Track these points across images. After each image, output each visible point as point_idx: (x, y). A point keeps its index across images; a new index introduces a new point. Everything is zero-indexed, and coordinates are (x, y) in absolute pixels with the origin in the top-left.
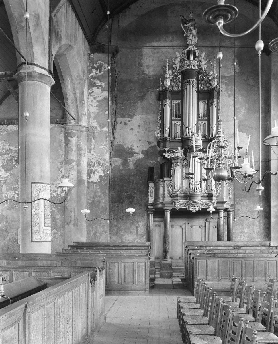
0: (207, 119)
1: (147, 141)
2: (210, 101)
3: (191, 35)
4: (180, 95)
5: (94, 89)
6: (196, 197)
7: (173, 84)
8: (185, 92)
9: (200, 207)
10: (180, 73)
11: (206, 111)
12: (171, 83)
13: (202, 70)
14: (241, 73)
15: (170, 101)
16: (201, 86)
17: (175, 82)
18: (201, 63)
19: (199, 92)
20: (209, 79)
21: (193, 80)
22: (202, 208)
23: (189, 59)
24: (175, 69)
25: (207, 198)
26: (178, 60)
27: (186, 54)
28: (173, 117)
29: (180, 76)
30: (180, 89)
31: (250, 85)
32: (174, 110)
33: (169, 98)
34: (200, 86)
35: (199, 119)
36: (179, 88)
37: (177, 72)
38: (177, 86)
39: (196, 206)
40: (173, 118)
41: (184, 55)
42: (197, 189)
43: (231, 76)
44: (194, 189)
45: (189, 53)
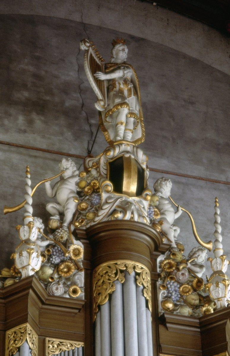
7: (49, 271)
8: (105, 309)
10: (76, 234)
16: (167, 298)
18: (162, 214)
19: (159, 320)
20: (195, 277)
23: (118, 188)
24: (57, 217)
26: (71, 186)
29: (78, 245)
30: (81, 294)
34: (160, 298)
36: (75, 292)
38: (69, 282)
41: (94, 172)
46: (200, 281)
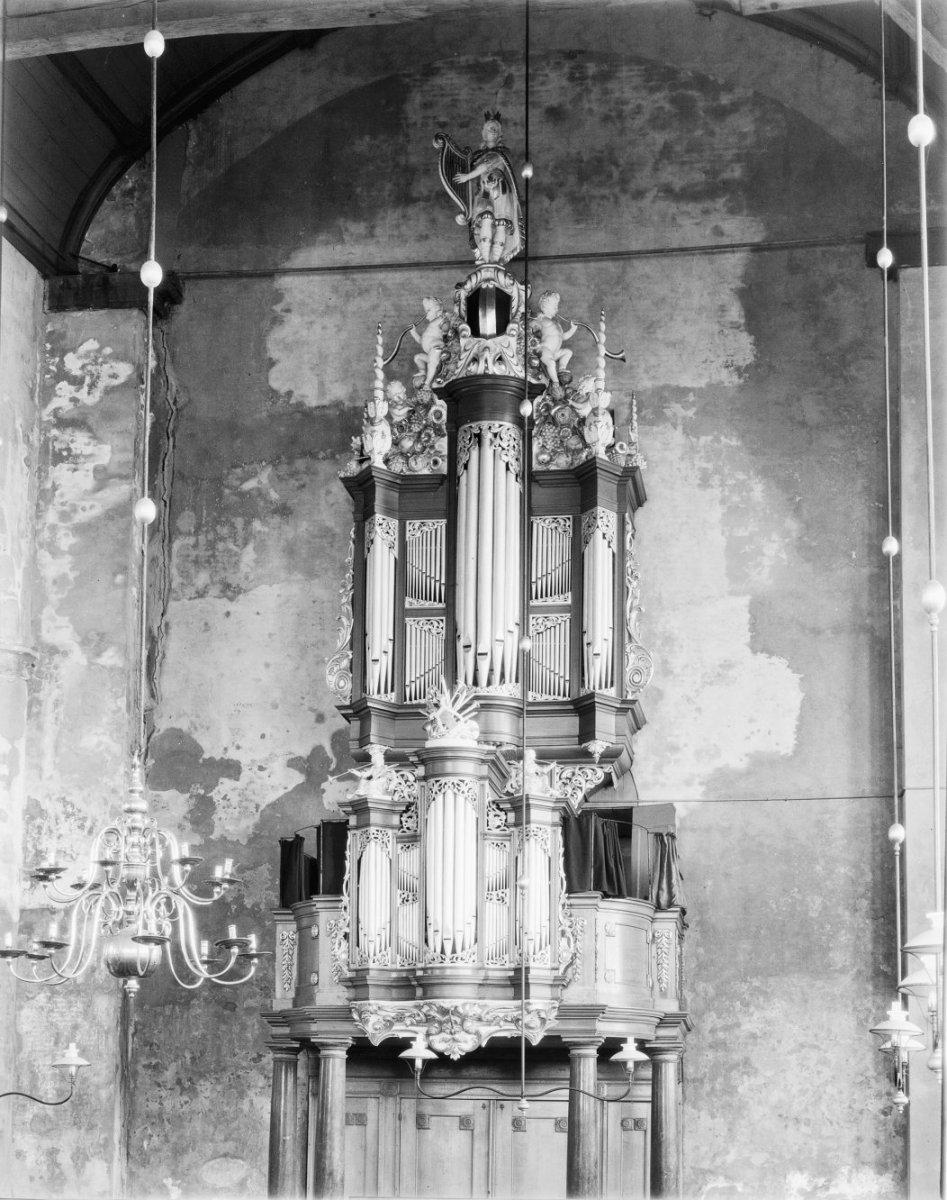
0: (569, 602)
1: (306, 707)
2: (585, 519)
3: (487, 222)
4: (438, 496)
5: (61, 473)
6: (447, 990)
8: (463, 480)
9: (477, 1034)
10: (441, 393)
11: (567, 566)
12: (396, 443)
13: (547, 375)
14: (755, 375)
15: (395, 523)
17: (420, 433)
19: (530, 478)
20: (577, 415)
21: (497, 424)
22: (493, 1041)
23: (476, 332)
25: (510, 992)
27: (463, 307)
28: (408, 599)
29: (441, 405)
31: (803, 424)
32: (416, 564)
33: (389, 512)
34: (535, 449)
35: (534, 603)
36: (436, 462)
37: (427, 387)
39: (456, 1028)
40: (410, 602)
42: (454, 951)
43: (710, 385)
44: (443, 952)
45: (475, 302)
46: (582, 421)
